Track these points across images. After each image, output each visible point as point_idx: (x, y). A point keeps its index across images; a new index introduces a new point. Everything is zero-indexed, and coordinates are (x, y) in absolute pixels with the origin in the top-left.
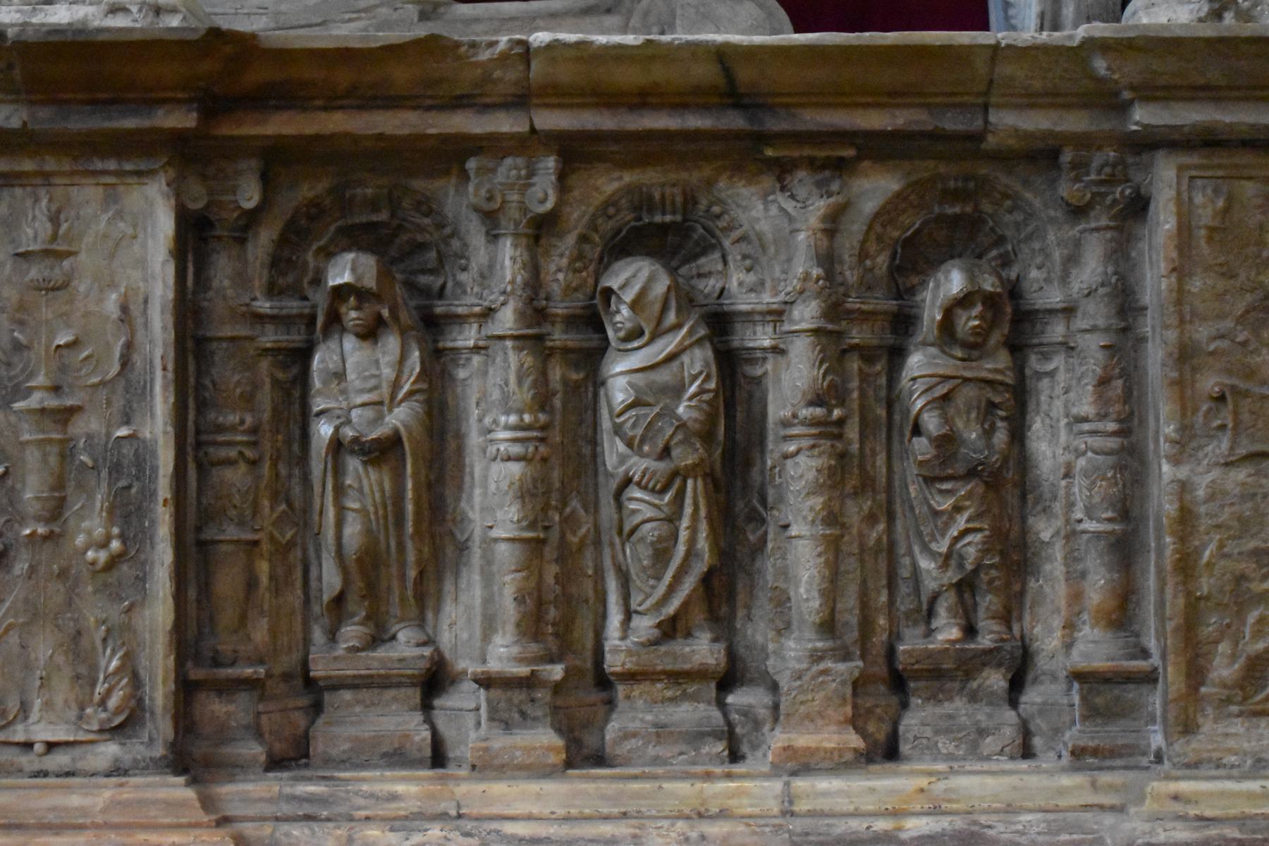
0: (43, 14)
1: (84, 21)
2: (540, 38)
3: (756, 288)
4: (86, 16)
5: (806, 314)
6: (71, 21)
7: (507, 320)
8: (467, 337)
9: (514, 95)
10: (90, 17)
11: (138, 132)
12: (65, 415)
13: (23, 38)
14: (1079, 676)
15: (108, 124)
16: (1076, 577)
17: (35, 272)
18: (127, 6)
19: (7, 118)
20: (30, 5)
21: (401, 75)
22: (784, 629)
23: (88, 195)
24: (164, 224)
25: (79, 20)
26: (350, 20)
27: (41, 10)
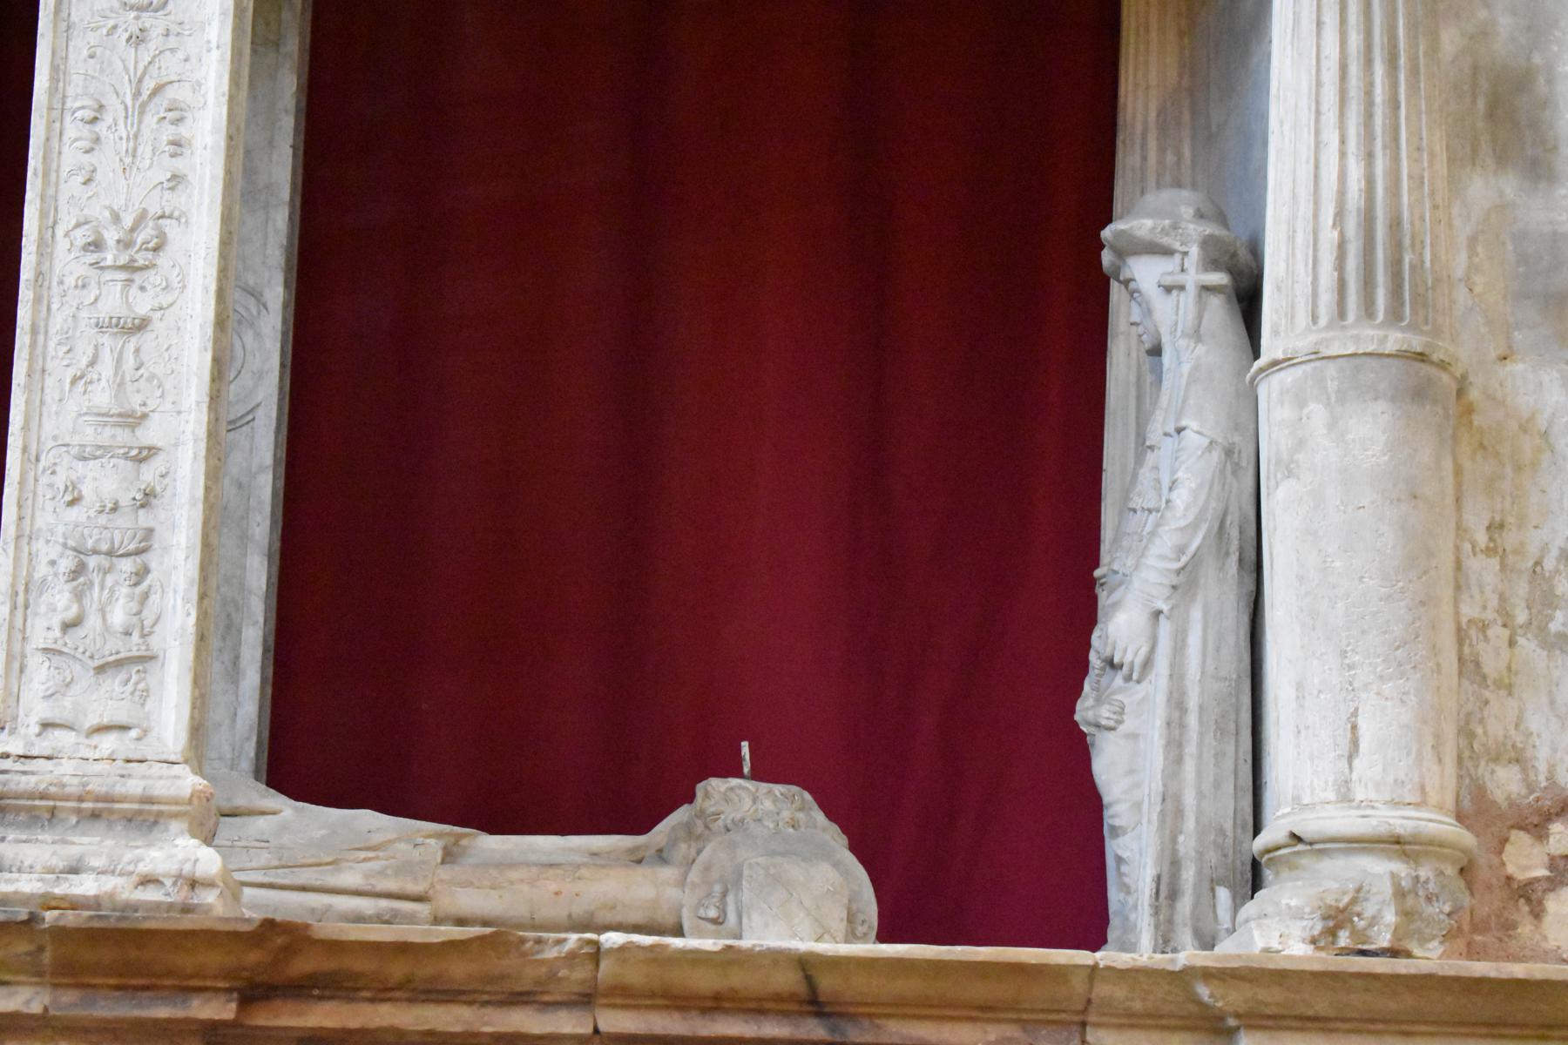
0: (67, 885)
1: (111, 895)
2: (613, 939)
4: (115, 888)
6: (98, 893)
9: (579, 994)
10: (119, 890)
11: (169, 1021)
13: (61, 923)
15: (137, 1013)
18: (161, 879)
19: (28, 1002)
20: (53, 873)
21: (459, 970)
25: (106, 893)
26: (365, 860)
27: (67, 879)
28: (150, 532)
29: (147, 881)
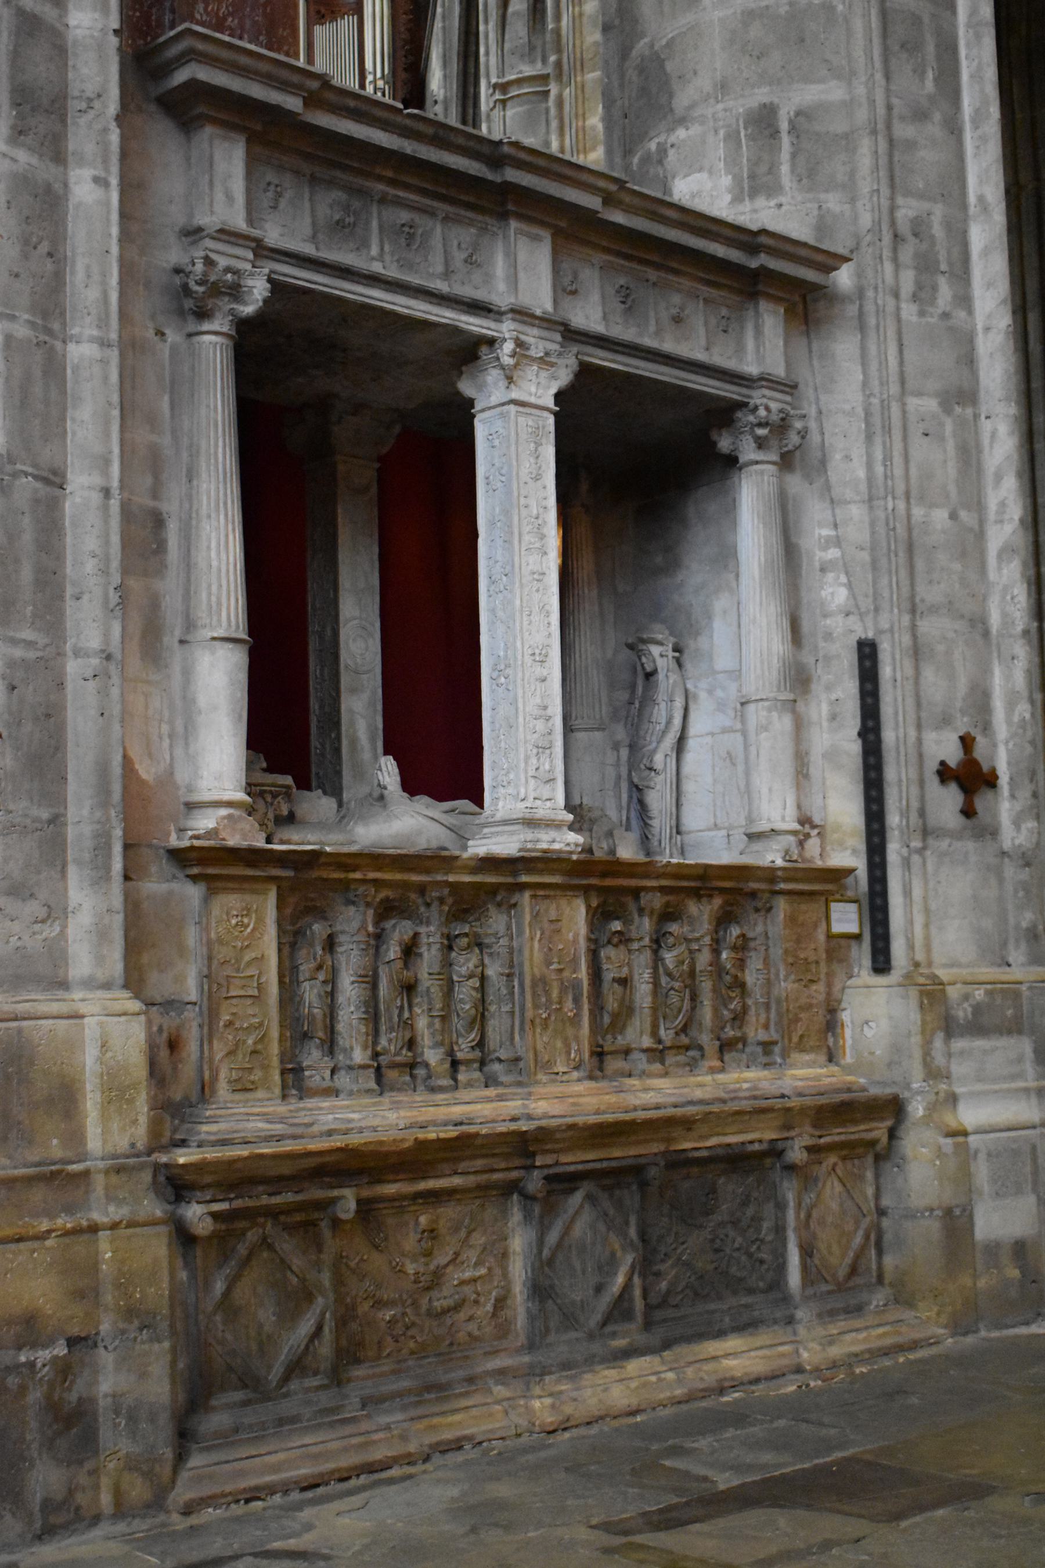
3: (693, 931)
5: (707, 940)
7: (647, 941)
8: (635, 946)
12: (560, 971)
14: (760, 1043)
16: (758, 1015)
17: (553, 927)
22: (701, 1032)
23: (563, 902)
24: (583, 910)
28: (551, 742)
29: (568, 844)
